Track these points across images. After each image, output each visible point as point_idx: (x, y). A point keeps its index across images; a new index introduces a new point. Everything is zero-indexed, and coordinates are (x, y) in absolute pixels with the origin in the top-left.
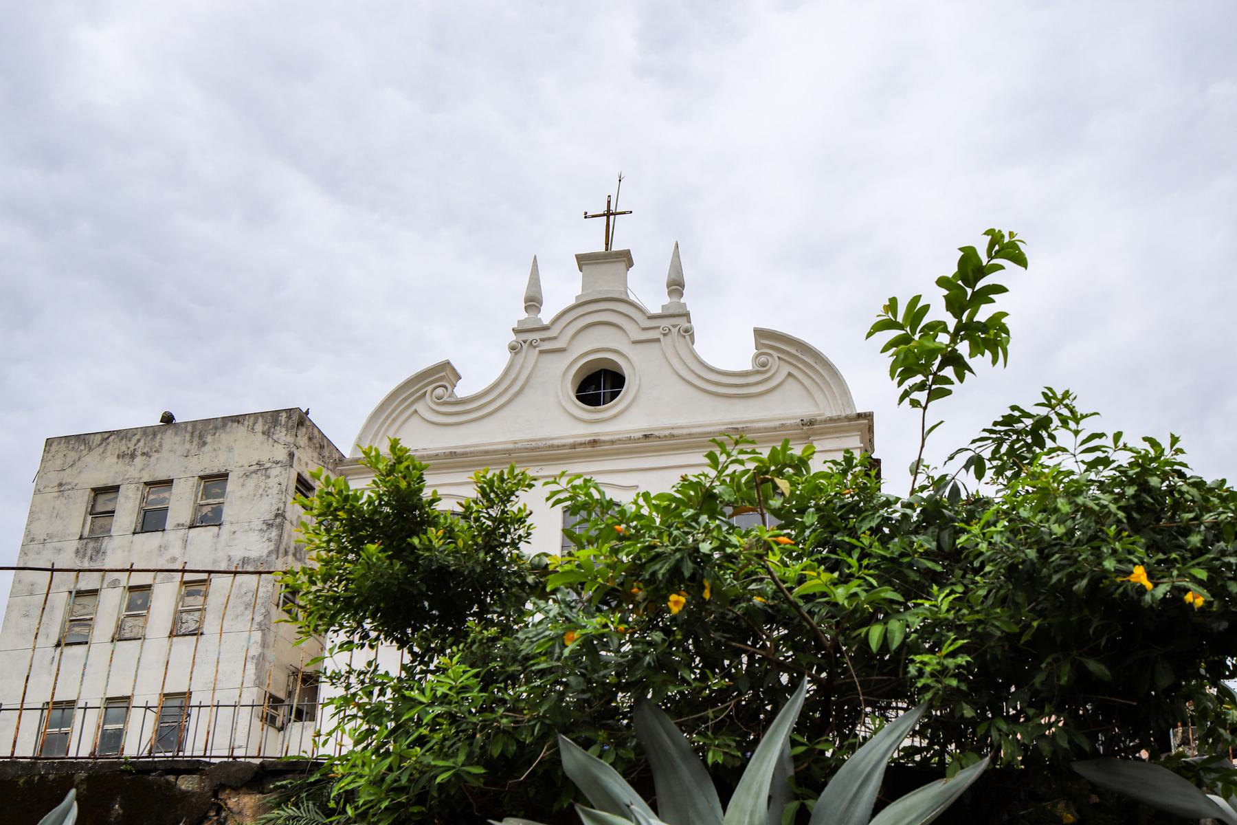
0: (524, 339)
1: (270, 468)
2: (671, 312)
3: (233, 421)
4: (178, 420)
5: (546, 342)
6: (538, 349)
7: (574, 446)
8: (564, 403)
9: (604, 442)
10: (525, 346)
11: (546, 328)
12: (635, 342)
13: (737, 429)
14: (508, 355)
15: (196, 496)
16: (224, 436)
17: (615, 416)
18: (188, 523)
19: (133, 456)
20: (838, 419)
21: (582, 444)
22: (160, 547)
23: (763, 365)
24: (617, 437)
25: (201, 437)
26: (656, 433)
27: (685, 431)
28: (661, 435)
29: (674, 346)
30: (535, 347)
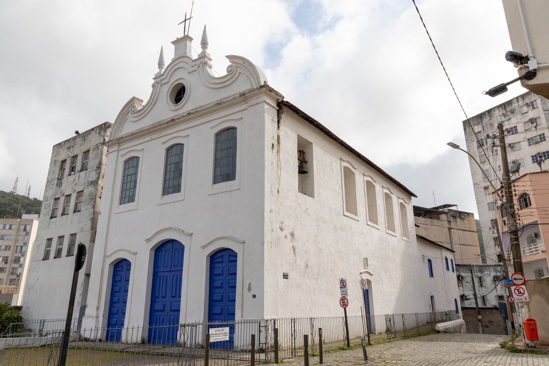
1: (99, 146)
3: (92, 130)
4: (80, 133)
7: (167, 123)
9: (176, 119)
11: (162, 75)
13: (218, 103)
14: (152, 89)
15: (83, 160)
16: (90, 136)
18: (80, 171)
19: (70, 148)
20: (253, 90)
21: (169, 122)
22: (74, 180)
24: (179, 116)
25: (85, 138)
28: (193, 112)
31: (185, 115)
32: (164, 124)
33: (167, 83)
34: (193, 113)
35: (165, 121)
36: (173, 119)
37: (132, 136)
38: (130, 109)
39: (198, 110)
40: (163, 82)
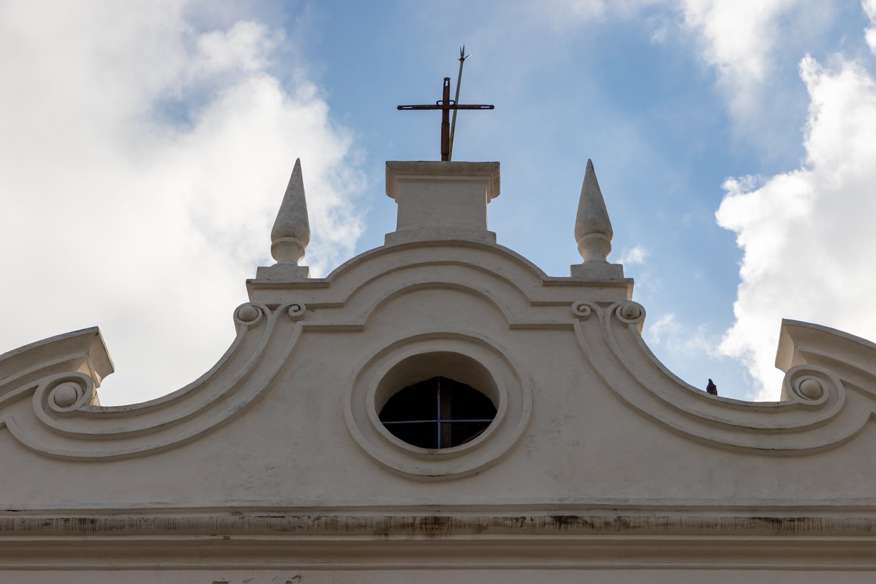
0: (271, 302)
2: (592, 276)
5: (319, 313)
6: (299, 325)
7: (385, 529)
8: (358, 436)
9: (460, 526)
10: (272, 317)
12: (515, 328)
17: (476, 473)
21: (404, 526)
23: (813, 395)
24: (491, 516)
26: (586, 515)
27: (654, 518)
28: (597, 522)
29: (606, 344)
30: (295, 320)
31: (537, 521)
32: (361, 527)
33: (357, 329)
34: (592, 526)
35: (381, 516)
36: (437, 521)
37: (68, 531)
38: (44, 382)
39: (631, 517)
40: (319, 319)
